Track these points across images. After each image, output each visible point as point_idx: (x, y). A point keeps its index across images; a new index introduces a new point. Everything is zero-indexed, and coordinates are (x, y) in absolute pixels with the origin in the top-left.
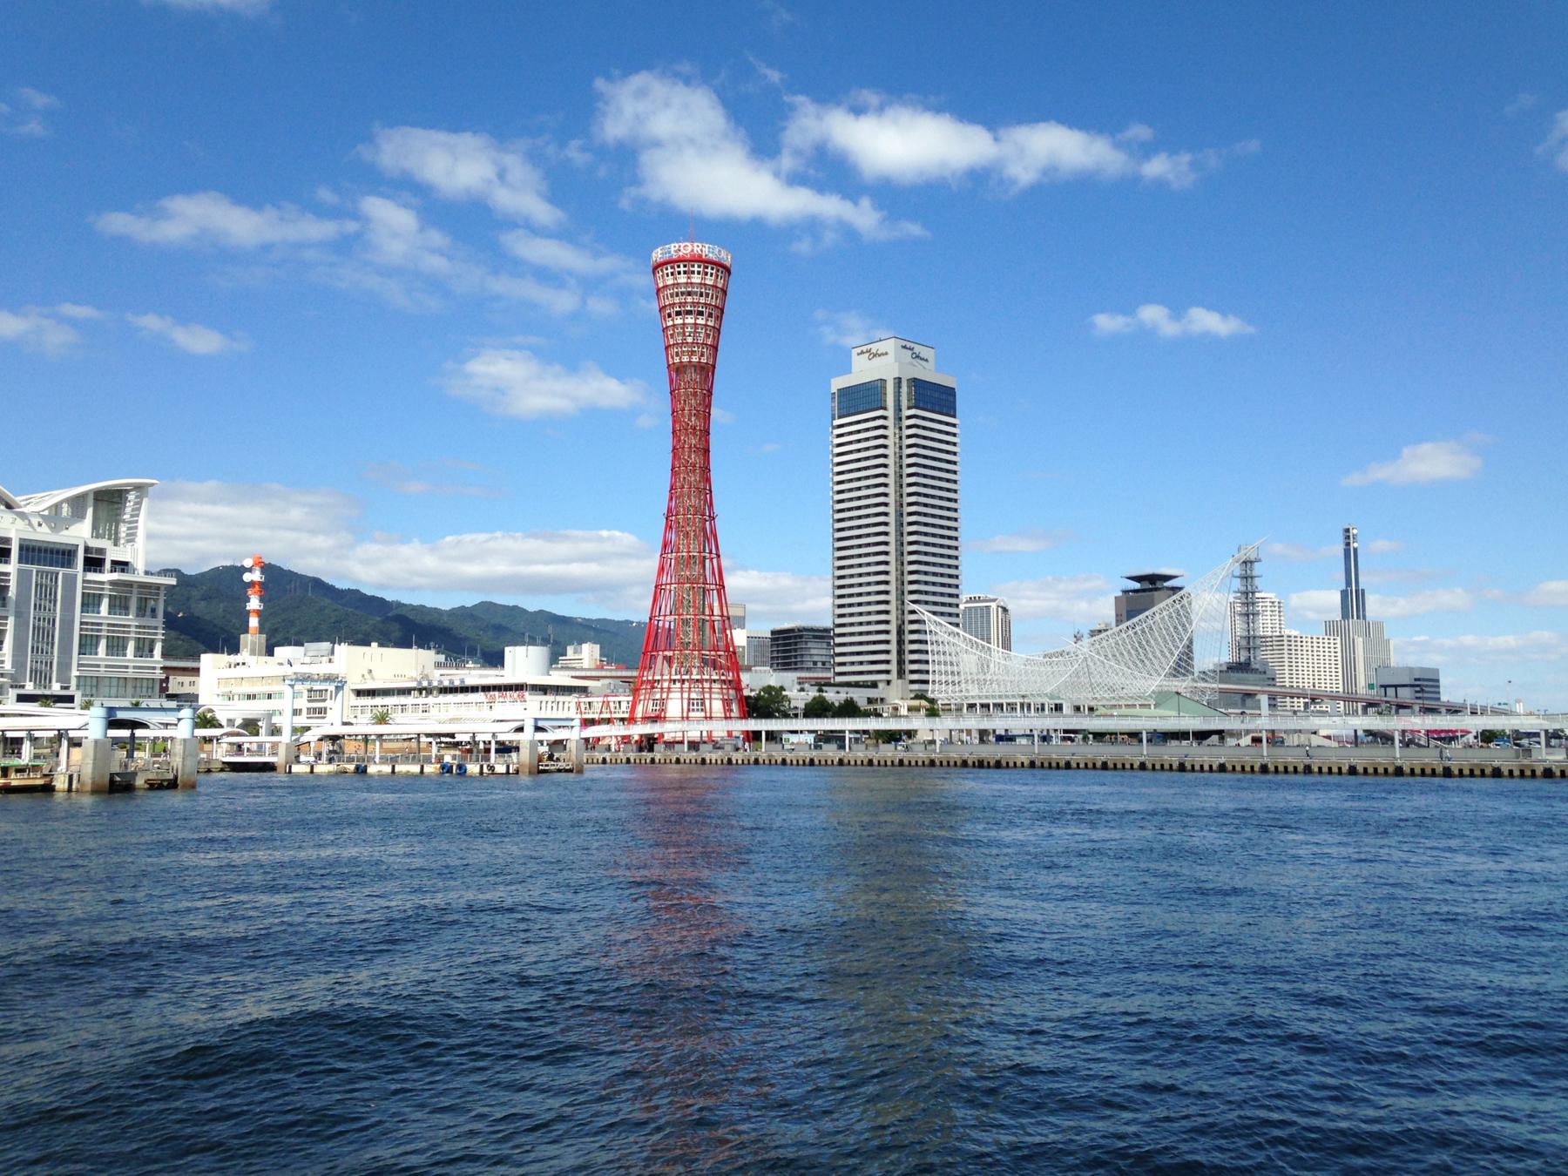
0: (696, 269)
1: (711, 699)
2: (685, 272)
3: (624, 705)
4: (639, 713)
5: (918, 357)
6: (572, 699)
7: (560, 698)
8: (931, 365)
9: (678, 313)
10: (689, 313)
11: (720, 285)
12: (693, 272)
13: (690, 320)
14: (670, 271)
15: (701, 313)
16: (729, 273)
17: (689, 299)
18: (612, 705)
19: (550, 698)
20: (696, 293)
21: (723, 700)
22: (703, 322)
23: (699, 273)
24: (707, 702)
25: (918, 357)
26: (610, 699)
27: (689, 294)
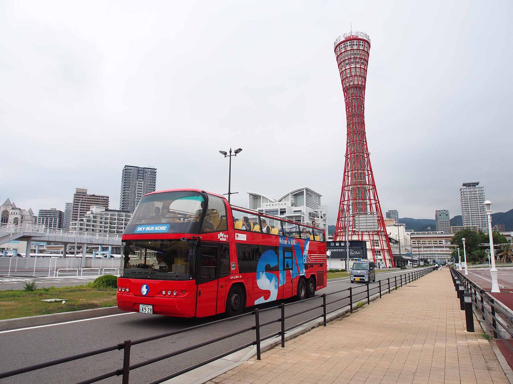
14: (348, 44)
15: (362, 63)
20: (361, 54)
22: (363, 67)
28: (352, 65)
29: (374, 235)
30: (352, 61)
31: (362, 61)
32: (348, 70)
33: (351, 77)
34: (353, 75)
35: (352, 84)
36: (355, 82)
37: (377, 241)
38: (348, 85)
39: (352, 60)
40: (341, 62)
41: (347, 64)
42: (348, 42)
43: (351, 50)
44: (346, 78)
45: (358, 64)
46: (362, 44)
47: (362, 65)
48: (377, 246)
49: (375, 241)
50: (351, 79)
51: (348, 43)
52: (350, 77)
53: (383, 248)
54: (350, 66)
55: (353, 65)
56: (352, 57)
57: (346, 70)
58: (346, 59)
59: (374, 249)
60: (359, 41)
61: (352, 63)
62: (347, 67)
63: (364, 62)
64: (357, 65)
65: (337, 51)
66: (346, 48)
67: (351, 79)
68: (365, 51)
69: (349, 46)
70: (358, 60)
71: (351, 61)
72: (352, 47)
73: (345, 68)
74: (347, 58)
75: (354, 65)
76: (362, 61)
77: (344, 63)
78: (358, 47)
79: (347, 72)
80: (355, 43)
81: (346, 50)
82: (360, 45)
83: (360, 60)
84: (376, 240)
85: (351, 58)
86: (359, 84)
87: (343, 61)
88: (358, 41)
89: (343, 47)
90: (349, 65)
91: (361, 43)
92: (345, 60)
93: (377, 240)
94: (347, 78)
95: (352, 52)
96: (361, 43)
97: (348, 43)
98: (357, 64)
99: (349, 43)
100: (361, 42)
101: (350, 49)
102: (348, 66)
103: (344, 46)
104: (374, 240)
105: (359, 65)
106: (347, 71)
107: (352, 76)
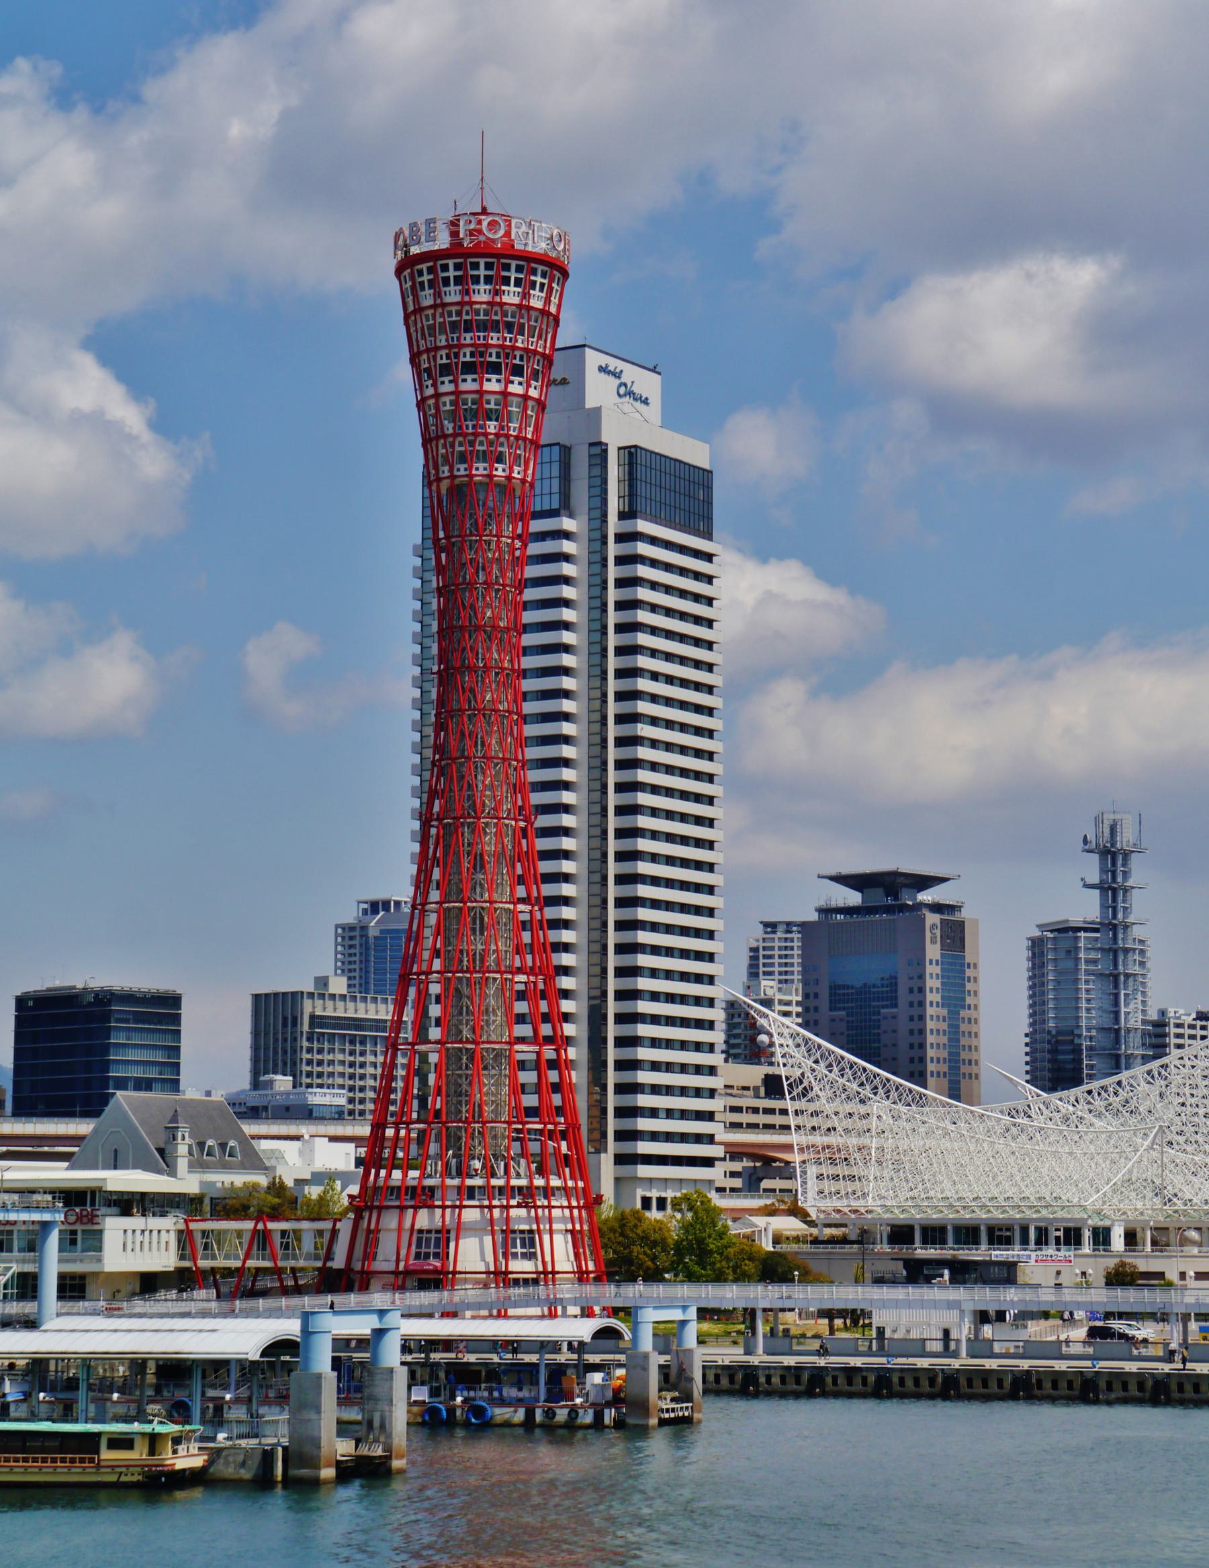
0: (513, 275)
1: (551, 1232)
2: (488, 280)
3: (308, 1244)
4: (380, 1265)
5: (630, 394)
6: (169, 1224)
7: (155, 1223)
8: (654, 412)
9: (469, 368)
10: (495, 368)
11: (553, 310)
12: (506, 281)
13: (492, 385)
15: (517, 371)
16: (565, 274)
17: (494, 339)
18: (277, 1239)
19: (136, 1222)
21: (573, 1232)
22: (519, 390)
23: (518, 283)
24: (546, 1238)
25: (630, 394)
26: (271, 1225)
27: (494, 326)
28: (464, 380)
31: (517, 362)
32: (447, 399)
33: (461, 439)
34: (470, 430)
35: (462, 472)
36: (476, 465)
37: (526, 1236)
38: (447, 474)
39: (468, 355)
41: (446, 370)
42: (451, 263)
43: (461, 304)
44: (437, 438)
45: (494, 377)
46: (516, 278)
47: (517, 379)
48: (524, 1256)
49: (518, 1235)
50: (458, 448)
51: (451, 267)
52: (455, 435)
54: (457, 386)
55: (469, 377)
56: (468, 341)
57: (437, 395)
58: (439, 344)
59: (507, 1273)
62: (443, 383)
63: (524, 363)
64: (489, 380)
66: (440, 293)
67: (458, 448)
68: (529, 308)
69: (455, 284)
71: (462, 359)
72: (467, 292)
73: (434, 385)
74: (444, 343)
75: (474, 380)
76: (515, 357)
77: (429, 362)
79: (443, 408)
80: (482, 272)
81: (438, 301)
83: (507, 356)
84: (522, 1232)
85: (461, 346)
86: (514, 478)
87: (428, 350)
89: (429, 281)
90: (451, 378)
92: (437, 348)
93: (531, 1232)
97: (451, 267)
98: (487, 376)
100: (513, 268)
101: (458, 298)
102: (446, 379)
103: (431, 277)
104: (514, 1232)
105: (498, 381)
106: (444, 404)
107: (465, 435)
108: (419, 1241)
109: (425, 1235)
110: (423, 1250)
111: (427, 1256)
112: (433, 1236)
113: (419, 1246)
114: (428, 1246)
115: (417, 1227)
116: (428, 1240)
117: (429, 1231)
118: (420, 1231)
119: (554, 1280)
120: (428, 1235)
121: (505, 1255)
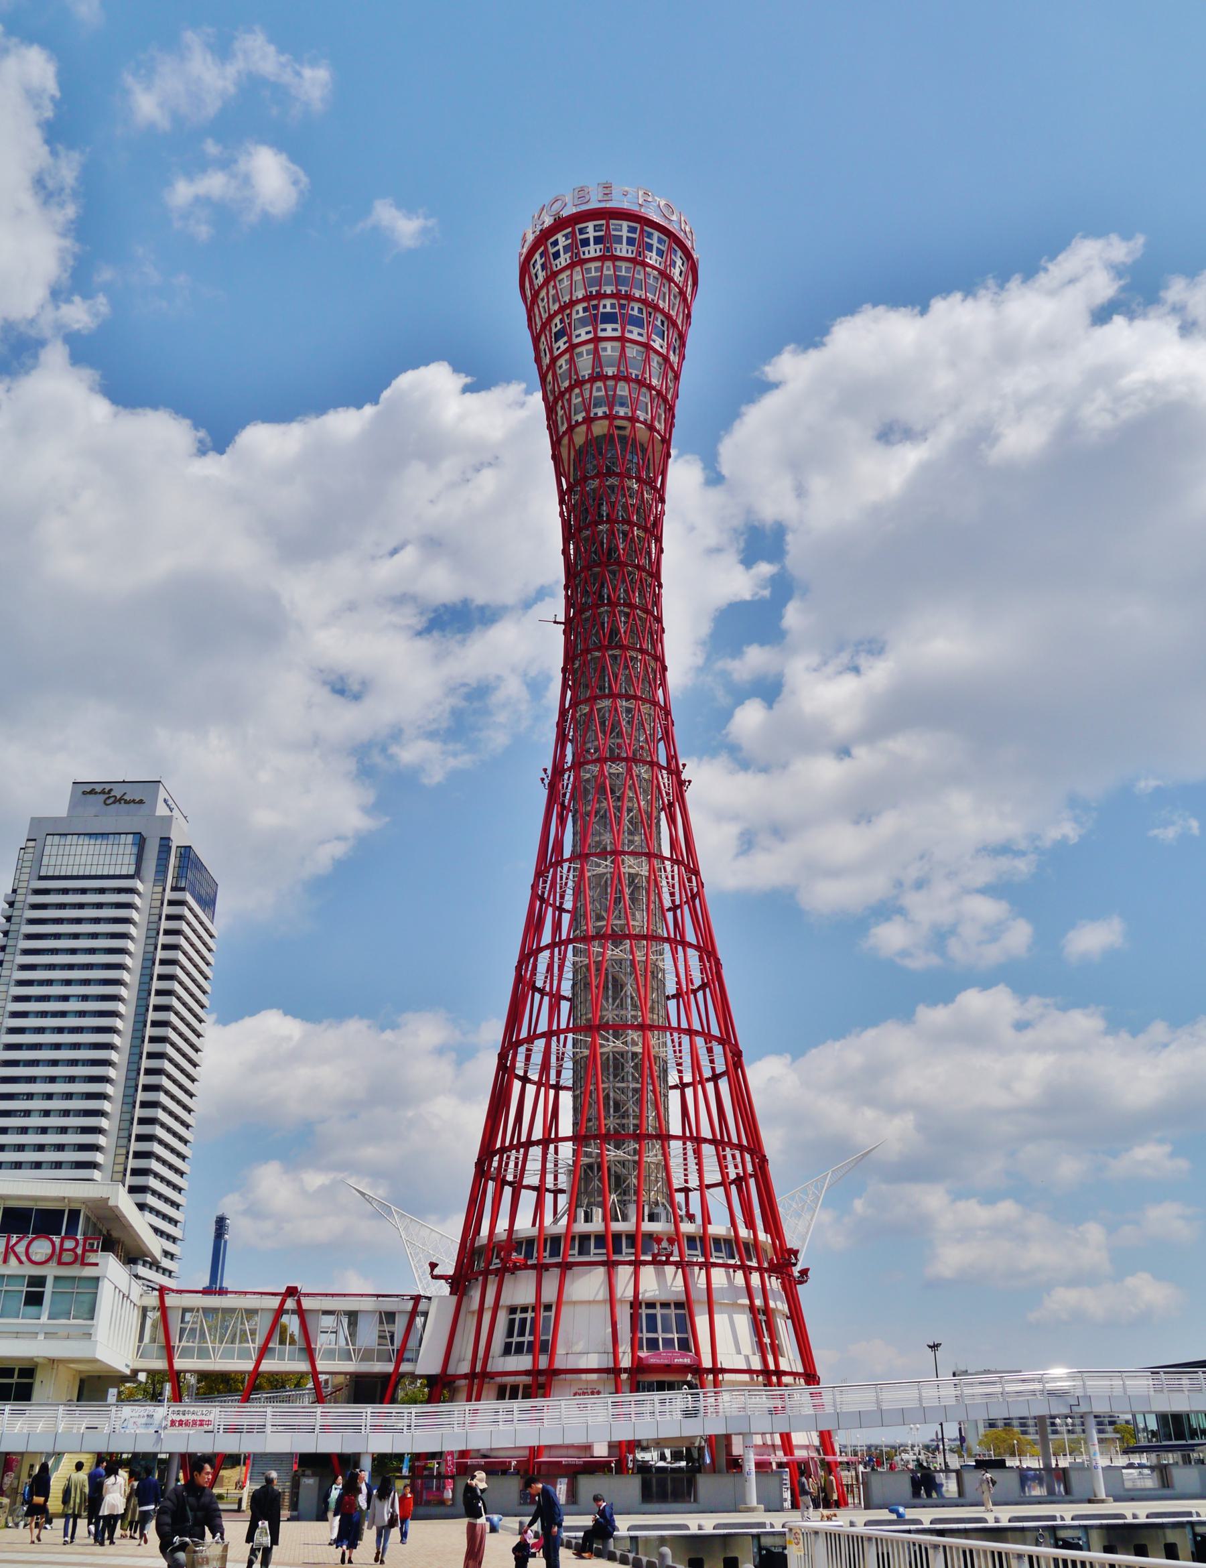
29: (645, 1263)
30: (608, 309)
40: (551, 317)
49: (658, 1311)
53: (772, 1367)
60: (646, 228)
61: (609, 318)
65: (533, 272)
70: (636, 310)
78: (639, 253)
82: (650, 247)
84: (665, 1305)
88: (638, 226)
91: (655, 242)
93: (679, 1305)
94: (577, 391)
95: (608, 269)
96: (655, 242)
99: (595, 231)
104: (651, 1305)
108: (512, 1322)
109: (518, 1316)
110: (516, 1339)
111: (519, 1349)
112: (529, 1315)
113: (510, 1334)
114: (522, 1334)
115: (506, 1300)
116: (523, 1321)
117: (524, 1309)
118: (513, 1310)
119: (716, 1384)
120: (524, 1315)
121: (635, 1345)
